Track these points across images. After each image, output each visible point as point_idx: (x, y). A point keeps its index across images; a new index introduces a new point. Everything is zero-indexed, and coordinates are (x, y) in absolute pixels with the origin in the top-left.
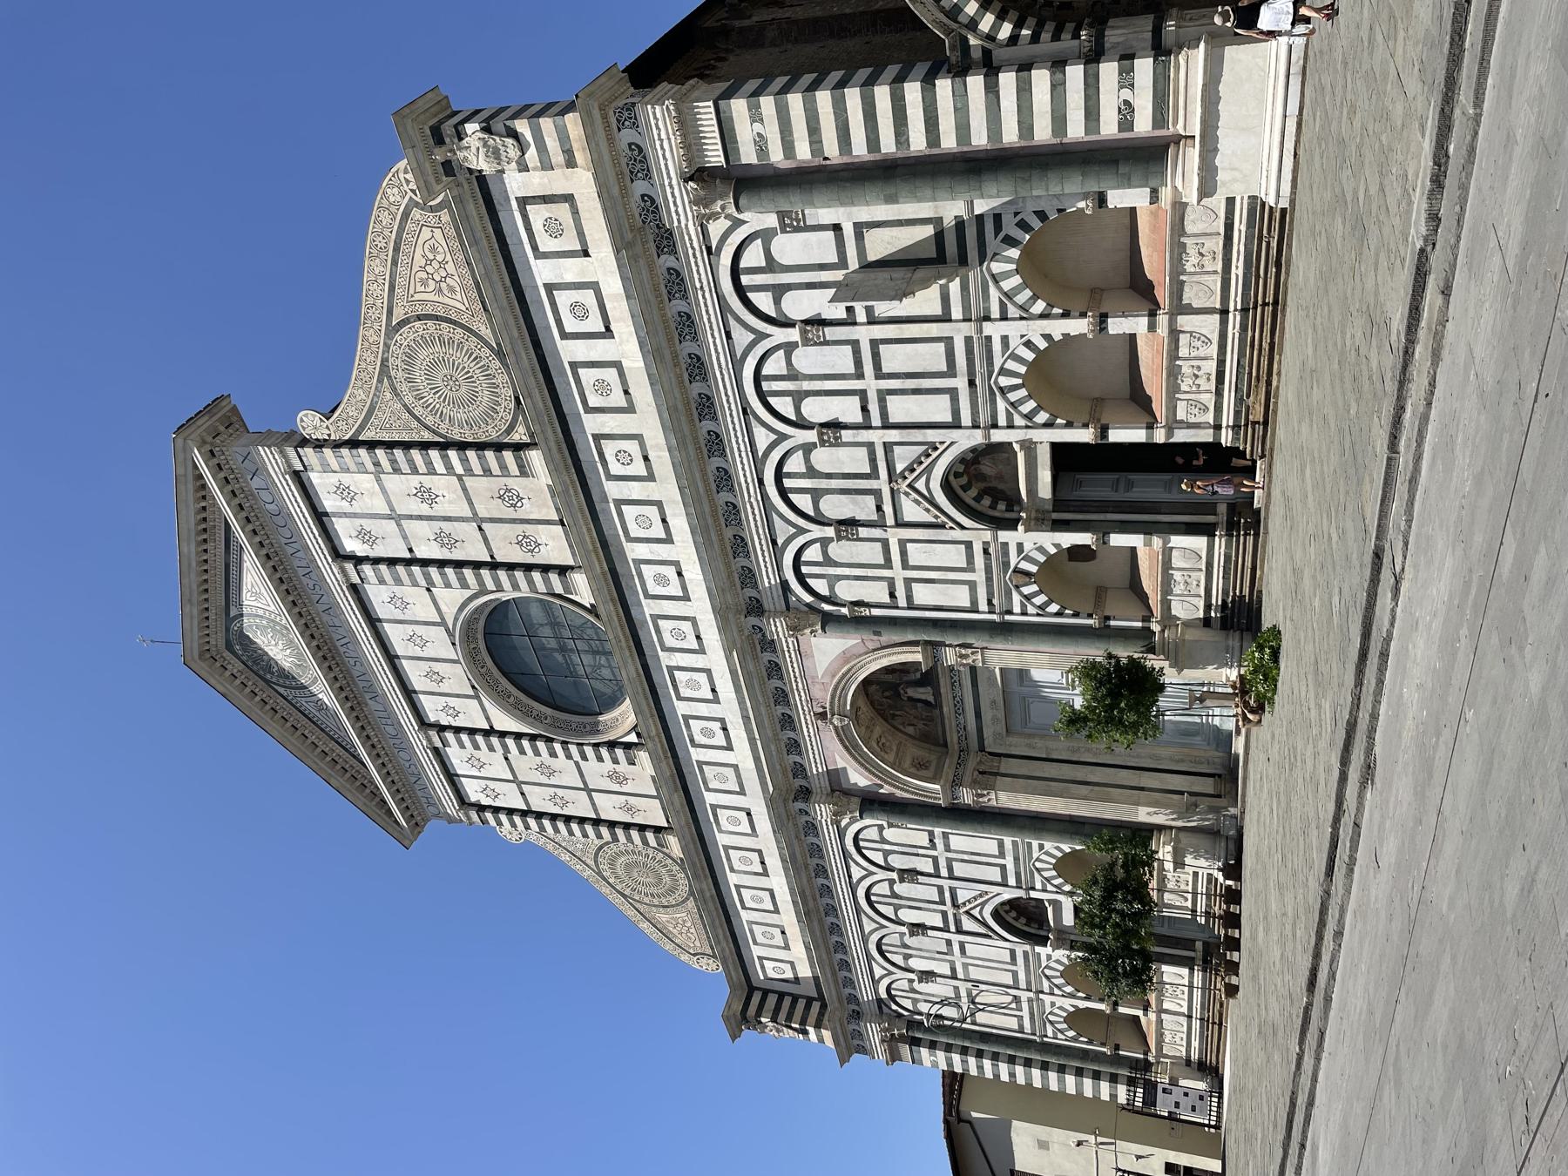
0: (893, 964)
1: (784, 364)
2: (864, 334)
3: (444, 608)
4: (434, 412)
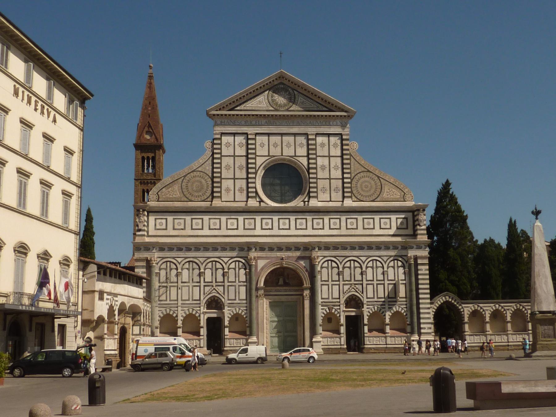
0: (183, 265)
1: (379, 266)
2: (387, 282)
3: (301, 158)
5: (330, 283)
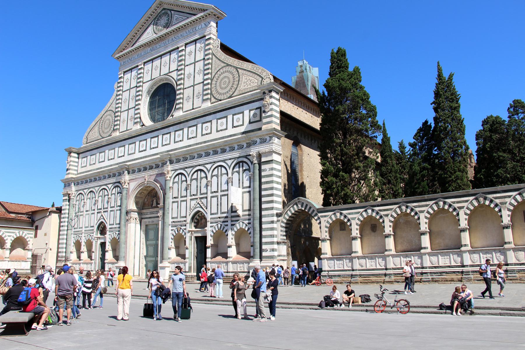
4: (219, 77)
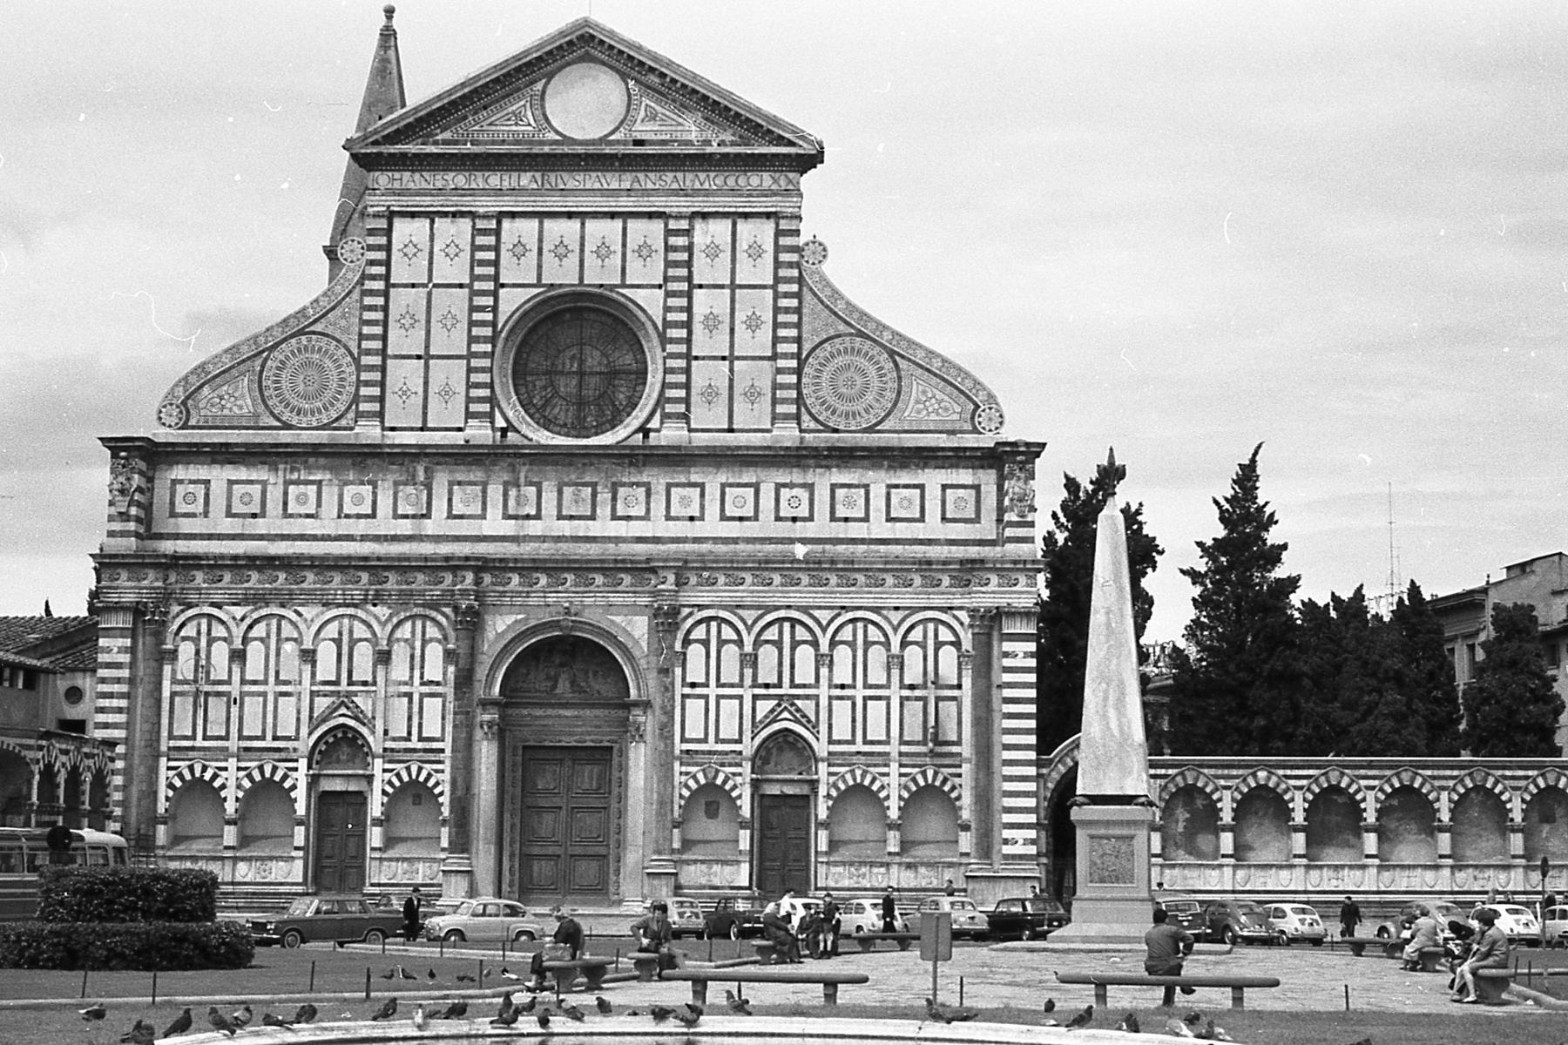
0: (250, 627)
1: (876, 639)
2: (895, 694)
4: (827, 360)
5: (712, 691)
